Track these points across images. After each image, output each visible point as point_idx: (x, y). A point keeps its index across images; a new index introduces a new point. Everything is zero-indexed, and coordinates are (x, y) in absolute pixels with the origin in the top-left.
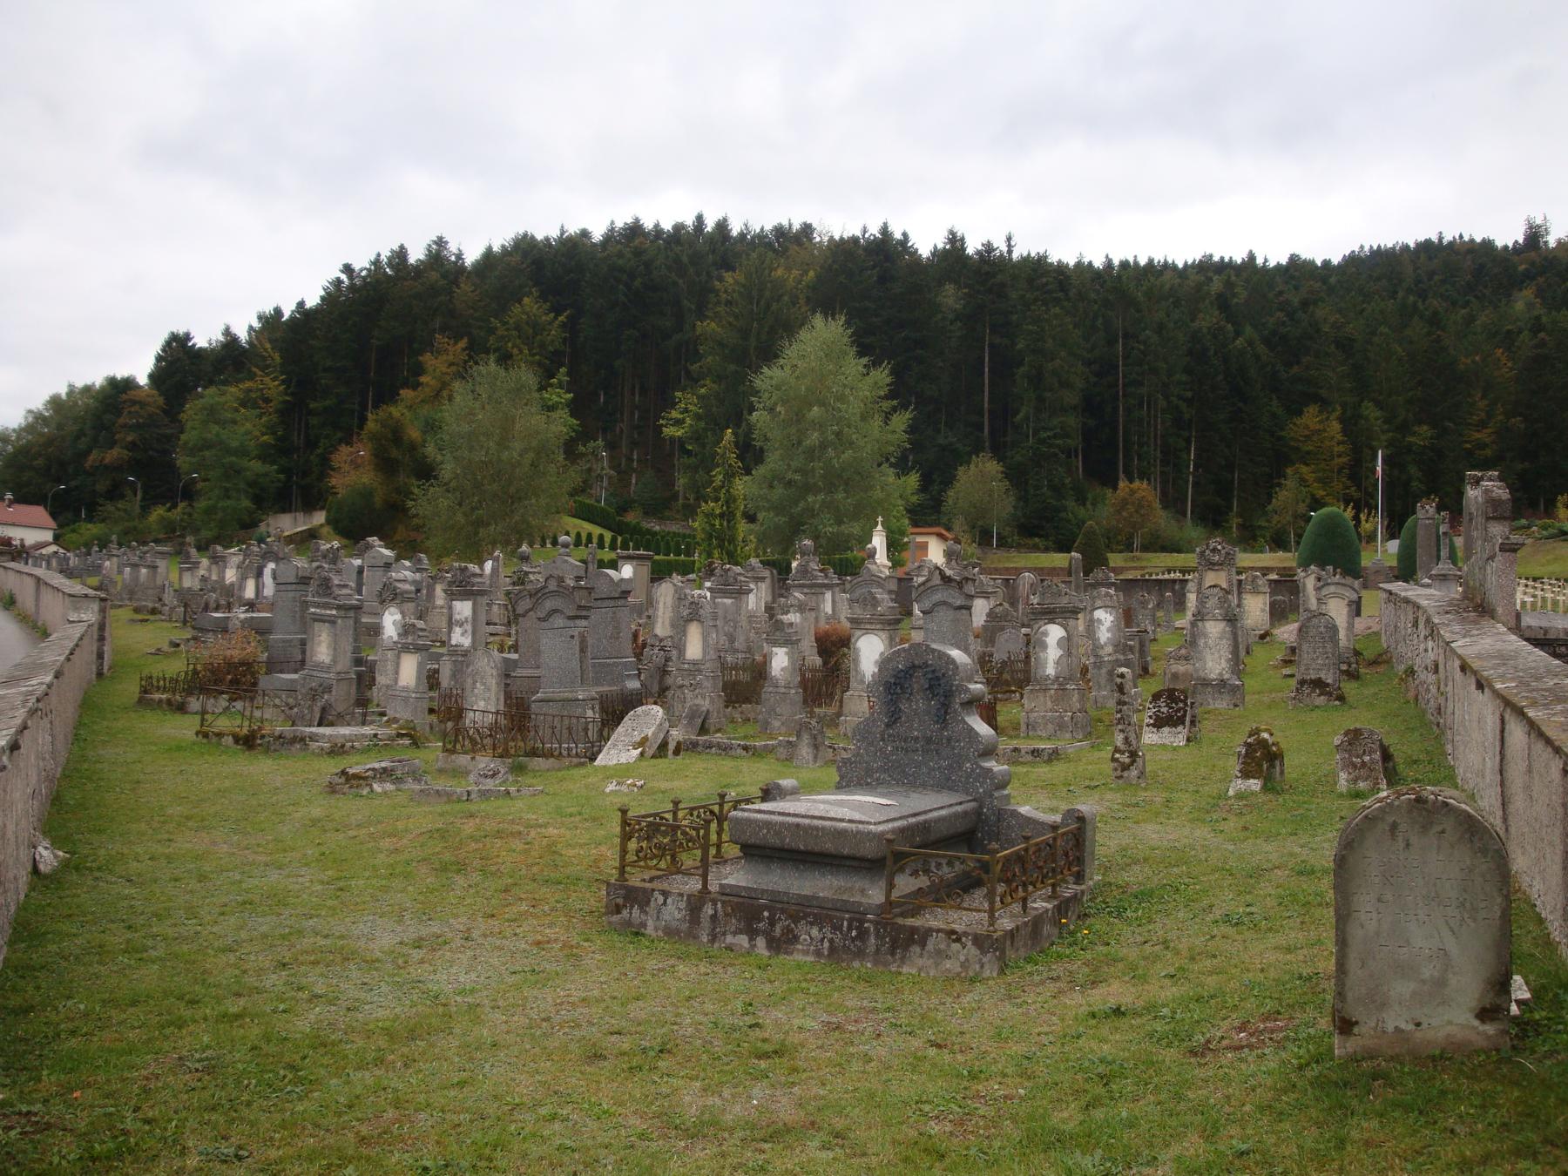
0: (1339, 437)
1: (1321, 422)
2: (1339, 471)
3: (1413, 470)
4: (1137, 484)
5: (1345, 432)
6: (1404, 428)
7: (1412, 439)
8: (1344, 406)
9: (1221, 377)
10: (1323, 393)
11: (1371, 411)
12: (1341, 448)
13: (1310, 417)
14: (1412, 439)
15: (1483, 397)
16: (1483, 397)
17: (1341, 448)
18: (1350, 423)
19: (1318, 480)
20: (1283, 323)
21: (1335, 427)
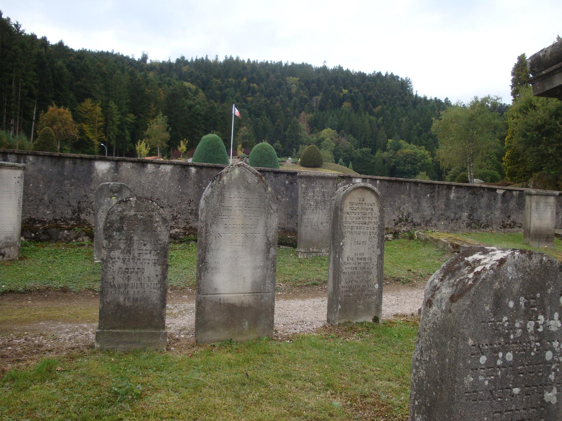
0: (100, 114)
1: (93, 106)
2: (99, 129)
3: (127, 132)
4: (62, 109)
5: (102, 111)
6: (124, 114)
7: (128, 119)
8: (102, 100)
9: (51, 77)
10: (93, 94)
11: (112, 104)
12: (100, 119)
13: (88, 103)
14: (128, 119)
15: (154, 107)
16: (154, 107)
17: (100, 119)
18: (105, 108)
19: (91, 131)
20: (73, 62)
21: (98, 109)
